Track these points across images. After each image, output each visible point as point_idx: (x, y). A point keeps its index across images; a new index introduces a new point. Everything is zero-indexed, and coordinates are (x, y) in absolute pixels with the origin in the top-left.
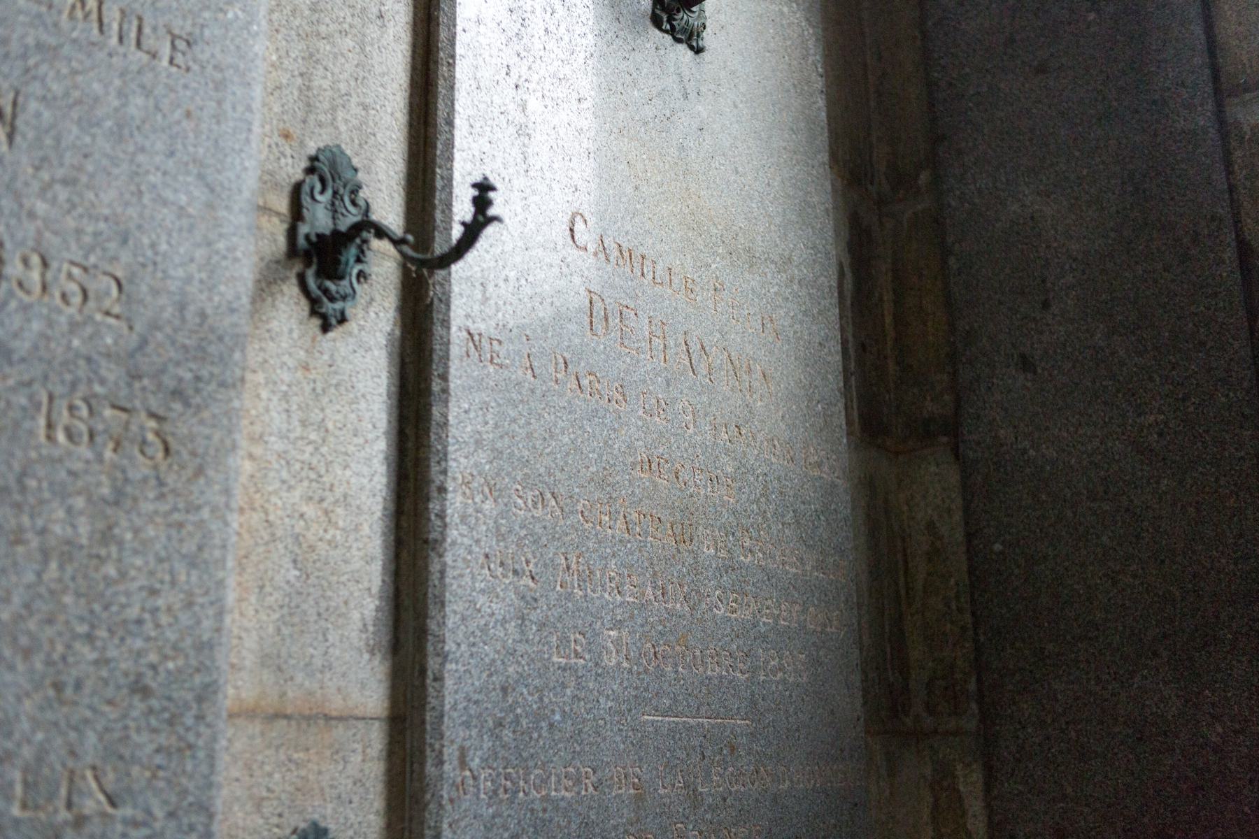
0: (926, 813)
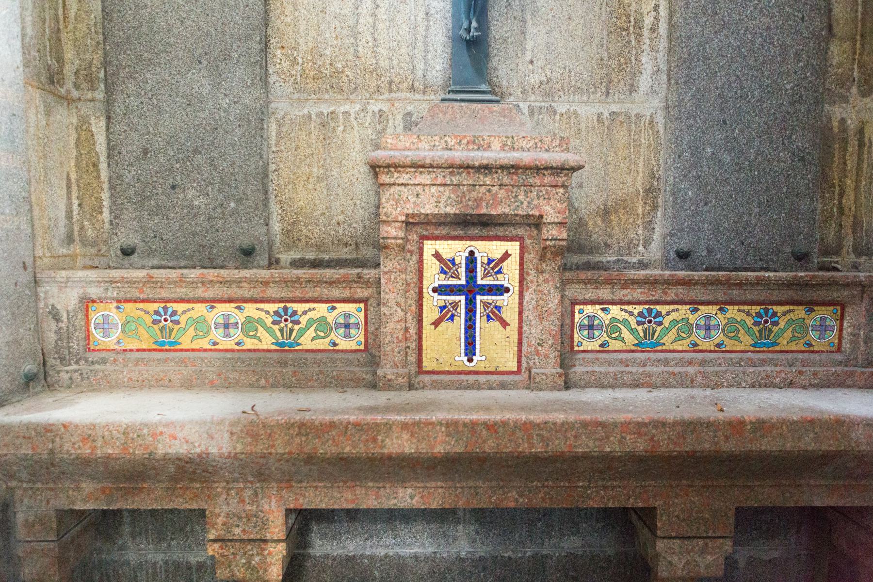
0: (72, 143)
